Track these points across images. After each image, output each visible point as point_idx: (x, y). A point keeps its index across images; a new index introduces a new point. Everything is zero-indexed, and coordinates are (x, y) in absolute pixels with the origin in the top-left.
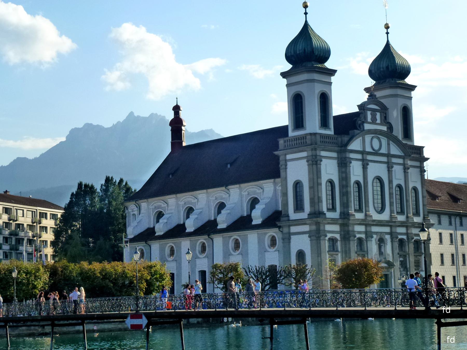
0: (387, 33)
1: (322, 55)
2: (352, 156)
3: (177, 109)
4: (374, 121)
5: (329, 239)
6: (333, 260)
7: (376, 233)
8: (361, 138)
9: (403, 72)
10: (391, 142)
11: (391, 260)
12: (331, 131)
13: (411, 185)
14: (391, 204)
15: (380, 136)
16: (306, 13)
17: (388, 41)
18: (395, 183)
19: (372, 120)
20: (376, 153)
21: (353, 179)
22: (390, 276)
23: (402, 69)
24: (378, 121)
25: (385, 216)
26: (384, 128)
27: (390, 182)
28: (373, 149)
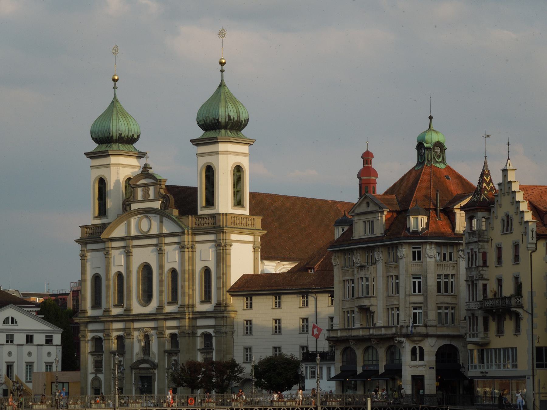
0: (222, 71)
1: (101, 136)
2: (114, 244)
3: (367, 157)
4: (146, 199)
5: (93, 339)
6: (99, 361)
7: (138, 329)
8: (125, 222)
9: (208, 122)
10: (164, 219)
11: (156, 361)
12: (108, 219)
13: (199, 267)
14: (161, 293)
15: (148, 215)
16: (115, 88)
17: (222, 81)
18: (167, 267)
19: (143, 198)
20: (145, 236)
21: (114, 270)
22: (153, 378)
23: (204, 118)
24: (151, 197)
25: (152, 307)
26: (157, 205)
27: (161, 267)
28: (141, 233)
